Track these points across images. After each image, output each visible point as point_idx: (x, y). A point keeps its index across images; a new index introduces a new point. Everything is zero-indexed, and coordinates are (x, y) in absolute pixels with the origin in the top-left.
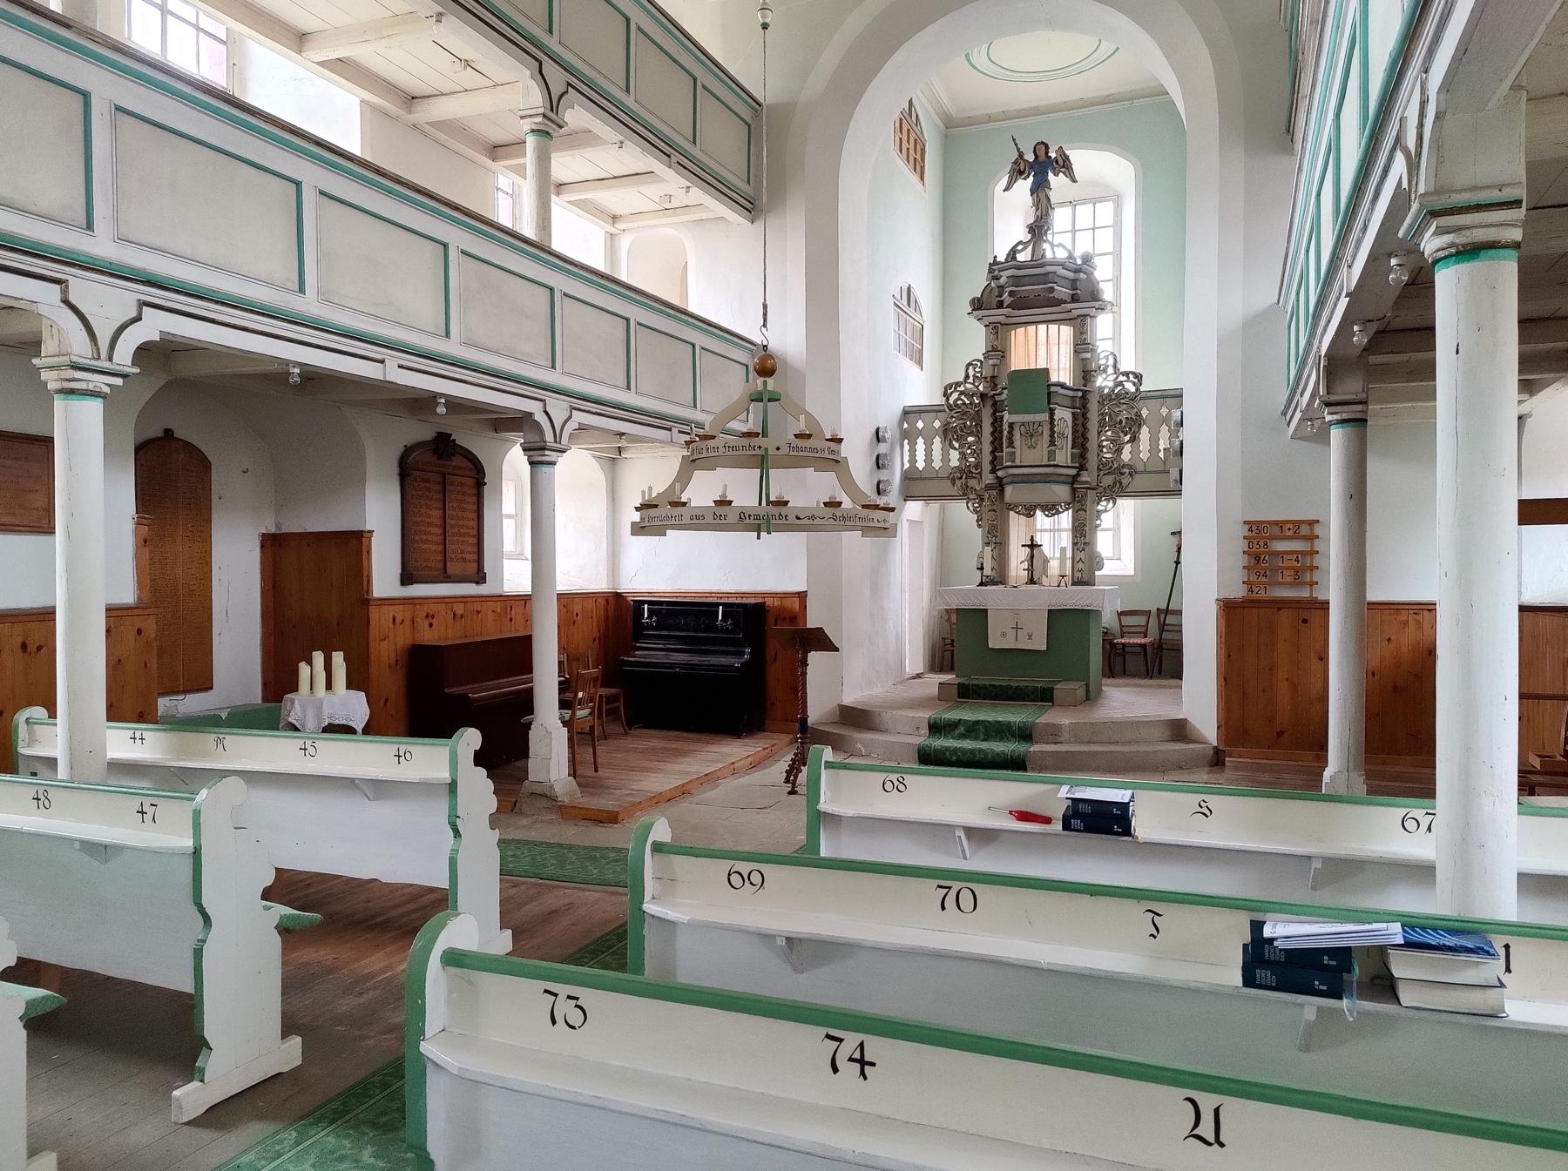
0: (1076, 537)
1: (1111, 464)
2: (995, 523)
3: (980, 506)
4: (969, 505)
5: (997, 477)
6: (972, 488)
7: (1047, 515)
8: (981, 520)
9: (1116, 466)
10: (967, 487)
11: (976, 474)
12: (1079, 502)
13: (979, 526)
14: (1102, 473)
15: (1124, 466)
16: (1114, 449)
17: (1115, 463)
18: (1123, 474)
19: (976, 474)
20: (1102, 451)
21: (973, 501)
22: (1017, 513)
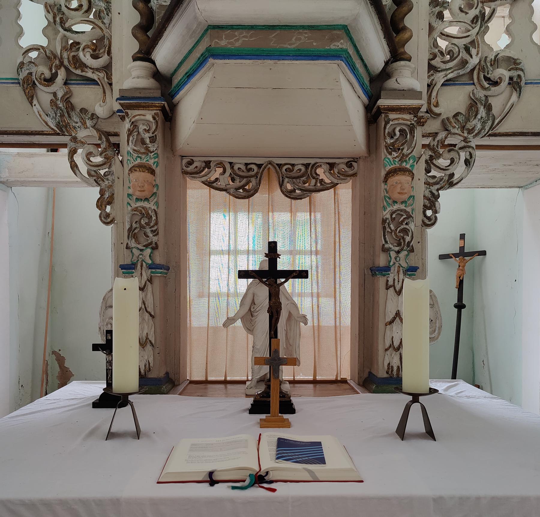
0: (386, 250)
1: (464, 55)
2: (150, 205)
3: (108, 161)
4: (79, 159)
5: (156, 75)
6: (83, 111)
7: (290, 194)
8: (109, 203)
9: (474, 61)
10: (70, 107)
11: (95, 70)
12: (391, 148)
13: (106, 219)
14: (440, 78)
15: (496, 62)
16: (473, 13)
17: (473, 51)
18: (496, 83)
19: (95, 70)
20: (440, 16)
21: (92, 149)
22: (210, 184)
